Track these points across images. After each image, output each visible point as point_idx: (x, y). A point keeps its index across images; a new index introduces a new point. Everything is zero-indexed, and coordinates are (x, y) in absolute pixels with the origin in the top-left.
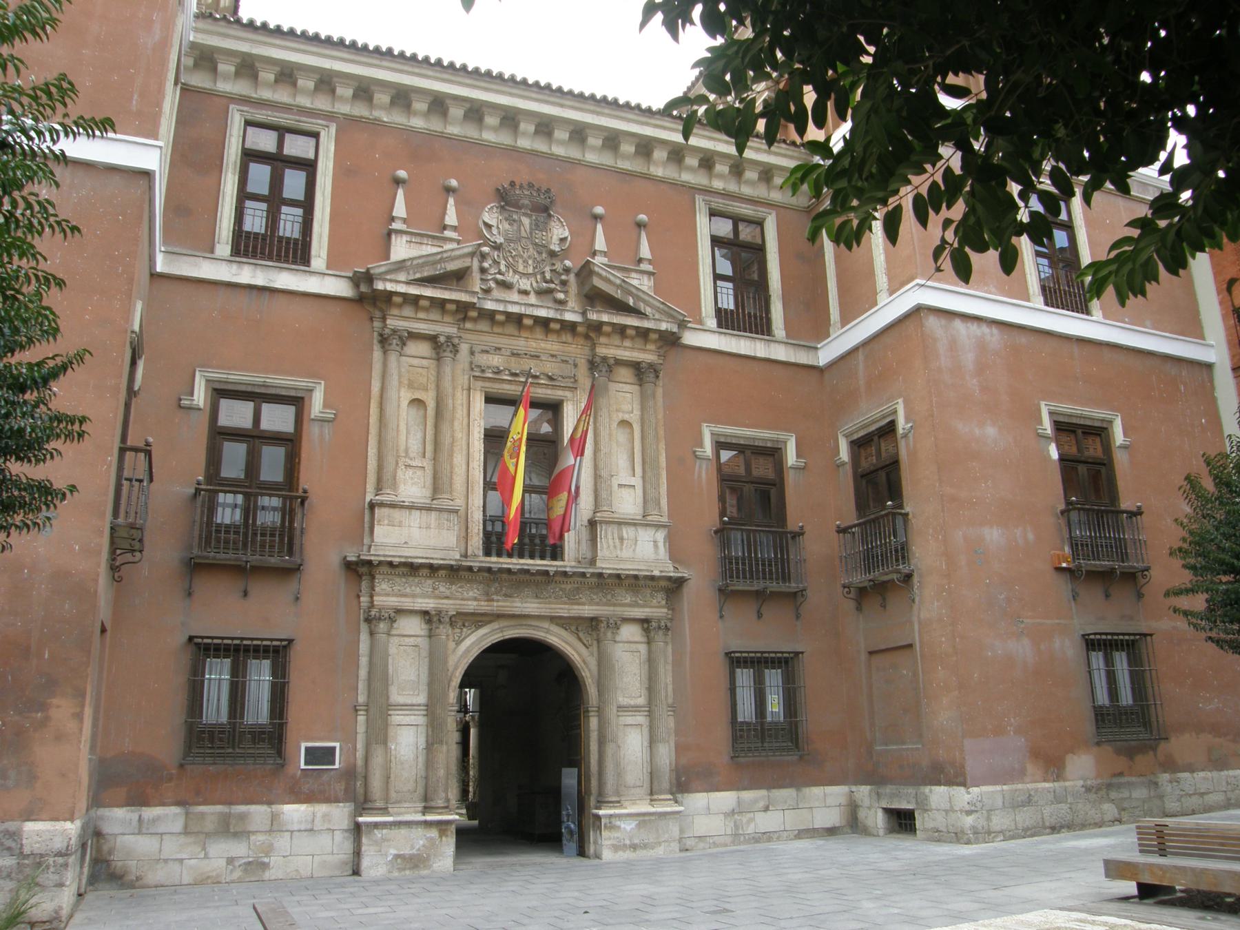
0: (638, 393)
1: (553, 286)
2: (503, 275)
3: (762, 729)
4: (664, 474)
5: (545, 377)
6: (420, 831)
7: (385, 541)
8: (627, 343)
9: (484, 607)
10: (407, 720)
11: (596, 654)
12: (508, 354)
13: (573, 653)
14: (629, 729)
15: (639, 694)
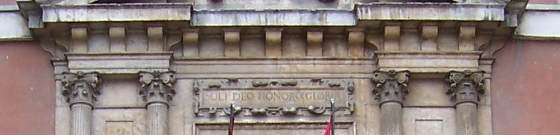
0: (452, 121)
8: (429, 47)
12: (249, 85)
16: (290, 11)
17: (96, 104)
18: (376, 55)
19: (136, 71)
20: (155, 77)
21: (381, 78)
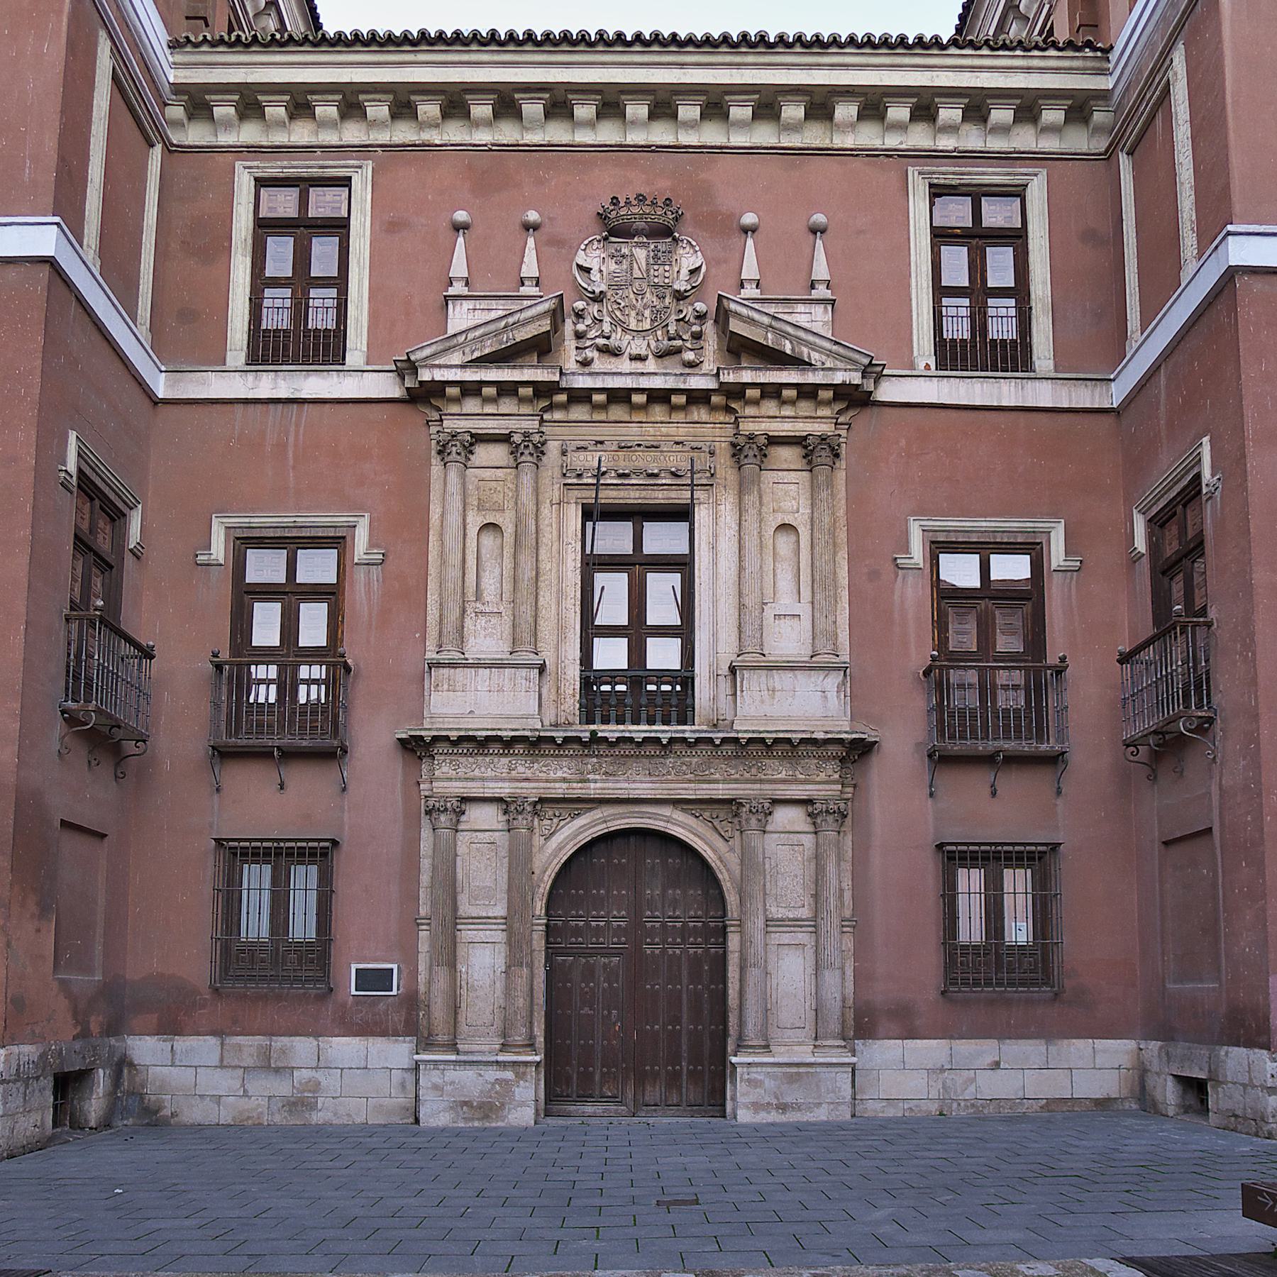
0: (807, 484)
1: (678, 343)
2: (608, 338)
3: (998, 955)
4: (845, 595)
5: (668, 475)
6: (492, 1074)
7: (444, 711)
8: (788, 411)
9: (577, 790)
10: (481, 936)
11: (738, 850)
13: (706, 848)
14: (785, 950)
15: (800, 904)
16: (655, 374)
17: (469, 464)
18: (736, 418)
19: (507, 432)
20: (525, 437)
21: (741, 440)
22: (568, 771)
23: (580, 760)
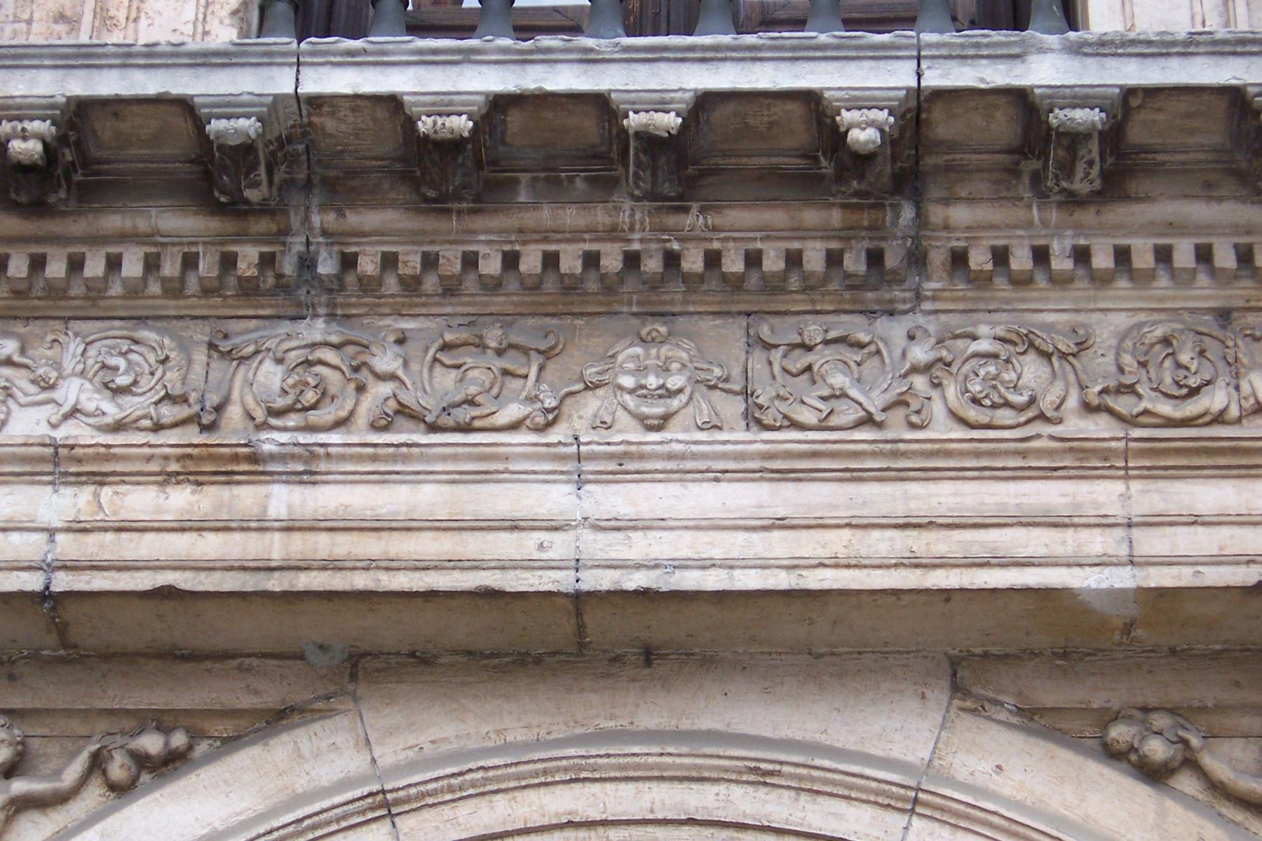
22: (94, 400)
23: (200, 333)
